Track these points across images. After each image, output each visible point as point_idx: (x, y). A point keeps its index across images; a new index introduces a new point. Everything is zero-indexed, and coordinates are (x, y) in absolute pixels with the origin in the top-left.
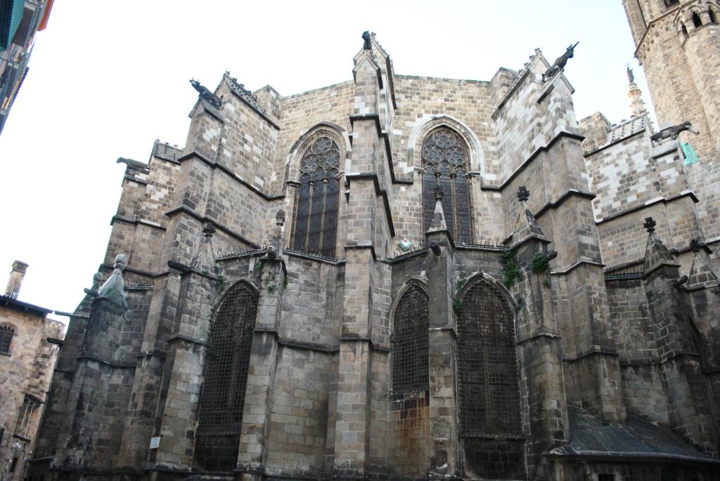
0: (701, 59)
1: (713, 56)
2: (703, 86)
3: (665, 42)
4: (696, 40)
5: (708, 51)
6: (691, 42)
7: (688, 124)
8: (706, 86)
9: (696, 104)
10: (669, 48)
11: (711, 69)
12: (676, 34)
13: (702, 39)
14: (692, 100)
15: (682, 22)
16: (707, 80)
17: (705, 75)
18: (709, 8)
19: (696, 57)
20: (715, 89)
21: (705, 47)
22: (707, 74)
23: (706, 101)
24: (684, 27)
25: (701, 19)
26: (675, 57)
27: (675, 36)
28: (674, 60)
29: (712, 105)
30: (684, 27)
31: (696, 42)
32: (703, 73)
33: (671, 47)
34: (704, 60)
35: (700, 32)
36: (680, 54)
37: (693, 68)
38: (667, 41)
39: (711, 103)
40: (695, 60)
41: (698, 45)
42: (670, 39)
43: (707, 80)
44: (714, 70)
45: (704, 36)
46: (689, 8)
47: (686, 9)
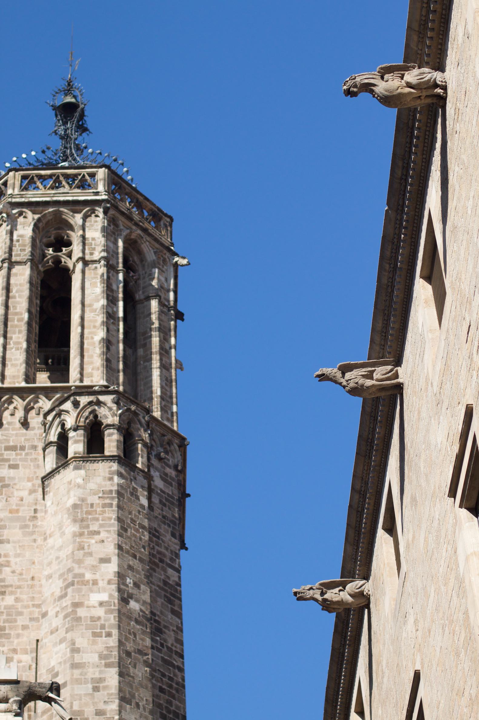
0: (75, 528)
1: (103, 535)
2: (58, 593)
3: (7, 448)
4: (80, 481)
5: (97, 519)
6: (66, 480)
7: (56, 688)
8: (66, 595)
9: (25, 627)
10: (11, 467)
11: (90, 561)
12: (41, 445)
13: (91, 486)
14: (20, 614)
15: (63, 425)
16: (73, 584)
17: (70, 570)
18: (129, 423)
19: (67, 521)
20: (81, 612)
21: (92, 505)
22: (77, 571)
23: (52, 633)
24: (63, 438)
25: (106, 439)
26: (16, 493)
27: (35, 447)
28: (14, 501)
29: (63, 645)
30: (63, 438)
31: (79, 486)
32: (70, 564)
33: (14, 467)
34: (81, 534)
35: (95, 465)
36: (32, 492)
37: (50, 541)
38: (13, 448)
39: (61, 642)
40: (60, 526)
41: (79, 493)
42: (22, 448)
43: (73, 584)
44: (94, 569)
45: (99, 480)
46: (90, 403)
47: (84, 400)
